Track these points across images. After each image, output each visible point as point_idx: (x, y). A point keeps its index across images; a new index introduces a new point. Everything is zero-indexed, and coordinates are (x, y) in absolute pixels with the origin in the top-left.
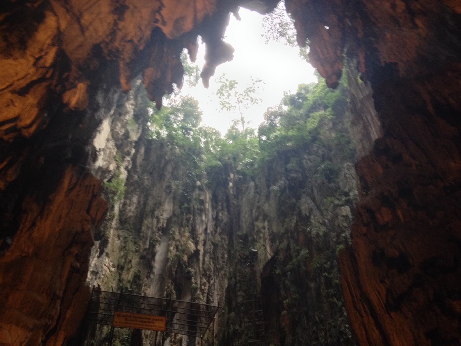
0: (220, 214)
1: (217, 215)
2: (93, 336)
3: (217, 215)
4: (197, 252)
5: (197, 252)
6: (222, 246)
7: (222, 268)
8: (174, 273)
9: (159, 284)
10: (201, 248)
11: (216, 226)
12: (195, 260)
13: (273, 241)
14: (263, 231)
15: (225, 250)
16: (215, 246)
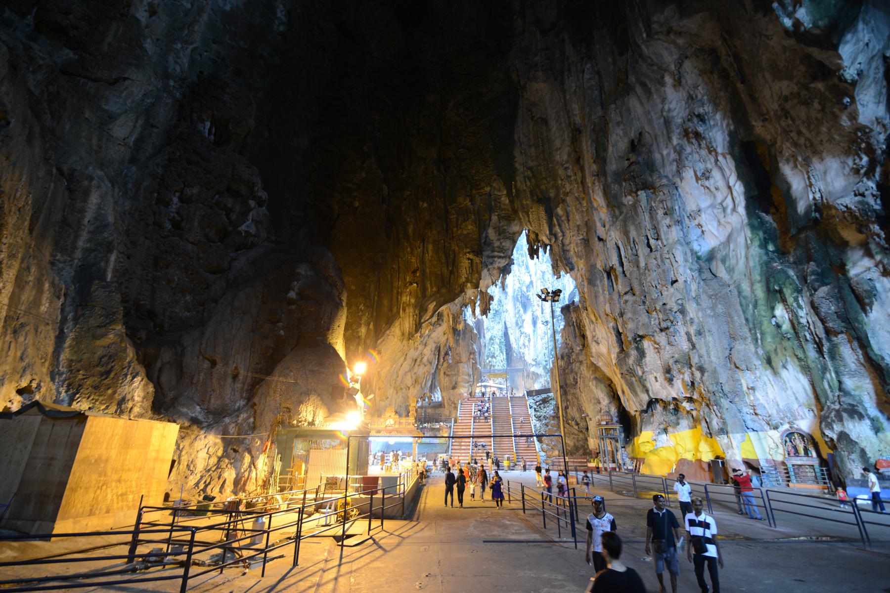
4: (531, 282)
5: (531, 282)
10: (534, 279)
16: (544, 273)
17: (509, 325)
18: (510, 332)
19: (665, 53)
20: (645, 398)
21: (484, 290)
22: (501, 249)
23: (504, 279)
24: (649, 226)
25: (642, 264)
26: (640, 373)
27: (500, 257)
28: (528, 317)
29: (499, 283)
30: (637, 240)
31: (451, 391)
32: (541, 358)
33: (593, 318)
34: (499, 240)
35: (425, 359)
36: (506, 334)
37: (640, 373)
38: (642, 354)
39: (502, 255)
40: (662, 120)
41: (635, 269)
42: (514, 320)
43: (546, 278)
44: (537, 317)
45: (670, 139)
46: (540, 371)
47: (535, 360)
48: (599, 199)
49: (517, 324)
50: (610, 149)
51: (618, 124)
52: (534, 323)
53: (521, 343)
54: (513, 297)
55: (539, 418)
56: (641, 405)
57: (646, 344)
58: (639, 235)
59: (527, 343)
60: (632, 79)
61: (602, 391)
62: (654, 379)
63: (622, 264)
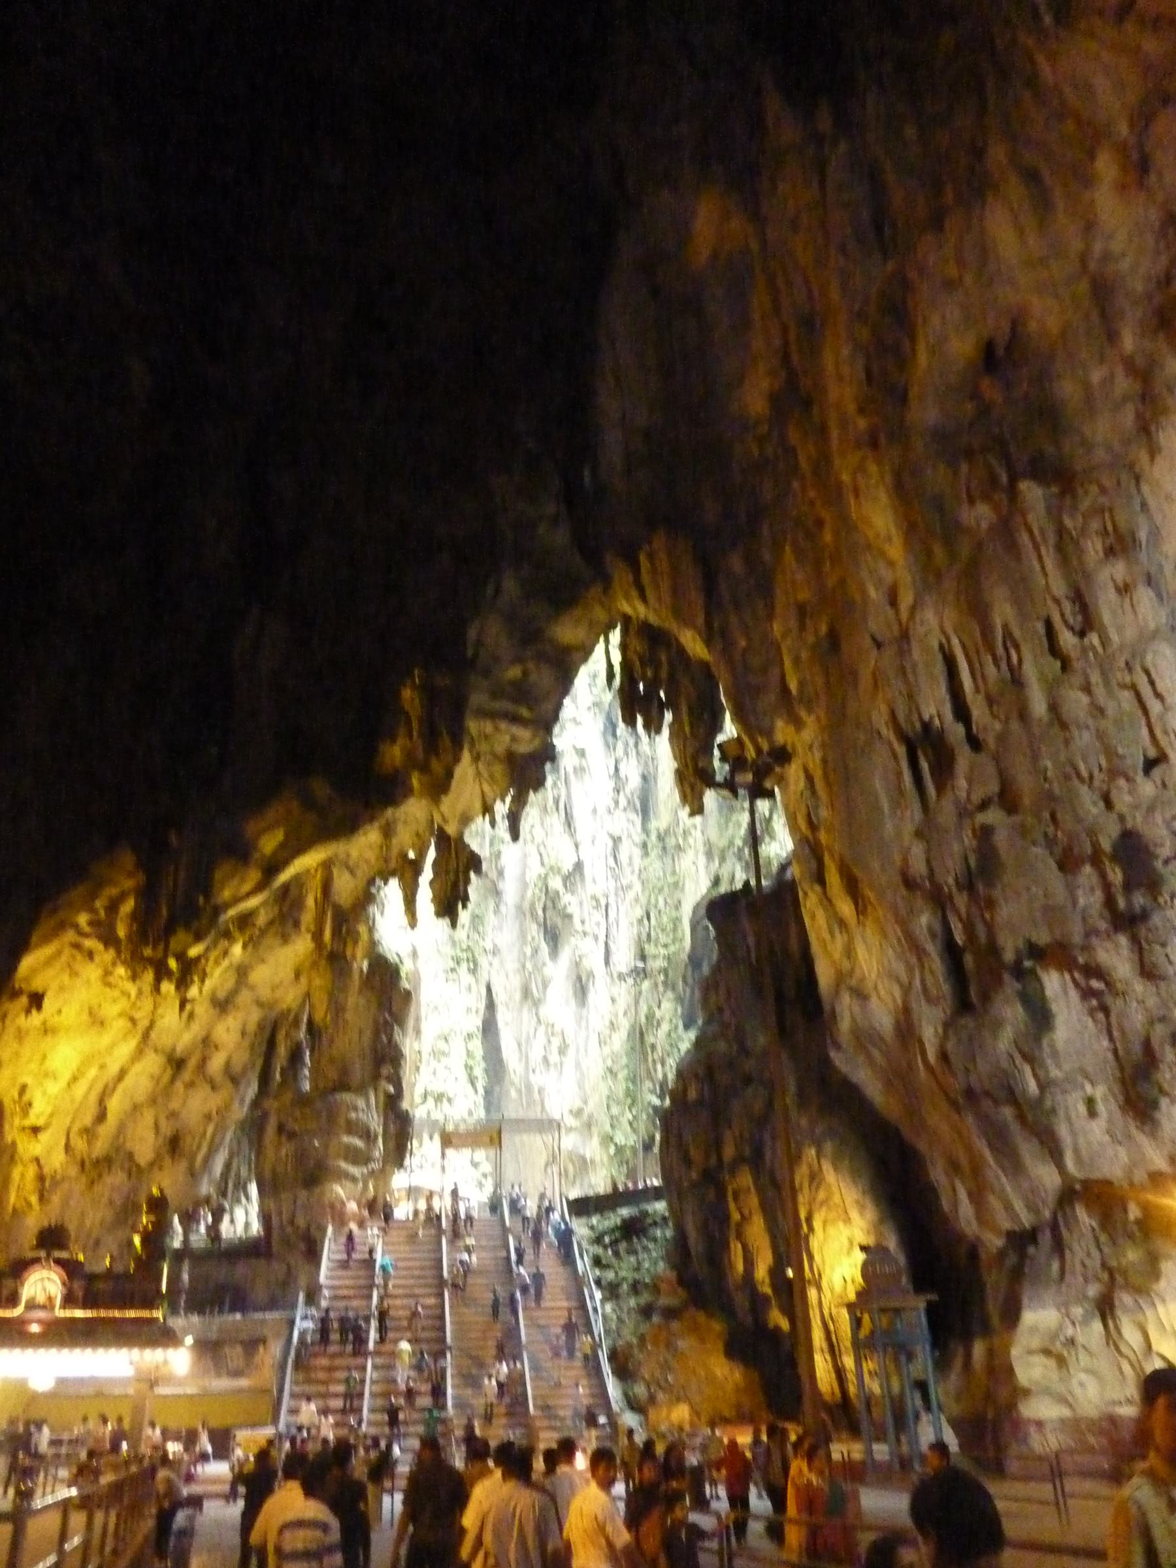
0: (622, 767)
1: (617, 769)
2: (418, 1032)
3: (617, 769)
4: (579, 866)
5: (579, 866)
6: (630, 836)
7: (629, 887)
8: (540, 912)
9: (517, 925)
11: (617, 791)
12: (578, 878)
13: (709, 855)
14: (693, 831)
15: (635, 845)
16: (616, 841)
17: (500, 997)
18: (503, 1016)
19: (1101, 84)
20: (1047, 1177)
21: (451, 830)
22: (522, 693)
23: (520, 802)
24: (1059, 587)
25: (1039, 706)
26: (1032, 1087)
27: (515, 719)
28: (558, 972)
29: (501, 809)
30: (1017, 633)
31: (303, 1194)
32: (596, 1105)
33: (846, 908)
34: (518, 660)
35: (216, 1063)
36: (489, 1028)
37: (1032, 1087)
38: (1040, 1017)
39: (525, 712)
40: (1084, 286)
41: (1015, 725)
42: (516, 982)
43: (623, 857)
44: (591, 975)
45: (1112, 336)
46: (593, 1149)
47: (578, 1113)
48: (879, 517)
49: (526, 993)
50: (923, 358)
51: (950, 285)
52: (581, 988)
53: (536, 1054)
54: (519, 908)
55: (612, 1291)
56: (1032, 1208)
57: (1053, 983)
58: (1023, 616)
59: (554, 1058)
60: (997, 153)
61: (855, 1175)
62: (1082, 1109)
63: (962, 712)
